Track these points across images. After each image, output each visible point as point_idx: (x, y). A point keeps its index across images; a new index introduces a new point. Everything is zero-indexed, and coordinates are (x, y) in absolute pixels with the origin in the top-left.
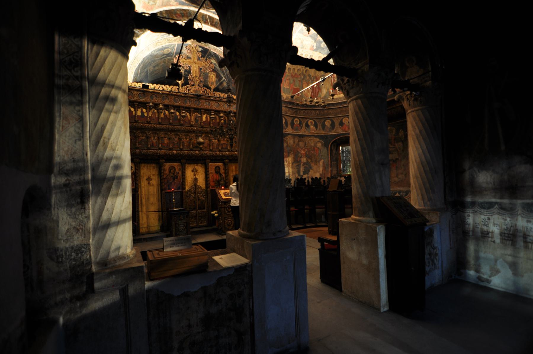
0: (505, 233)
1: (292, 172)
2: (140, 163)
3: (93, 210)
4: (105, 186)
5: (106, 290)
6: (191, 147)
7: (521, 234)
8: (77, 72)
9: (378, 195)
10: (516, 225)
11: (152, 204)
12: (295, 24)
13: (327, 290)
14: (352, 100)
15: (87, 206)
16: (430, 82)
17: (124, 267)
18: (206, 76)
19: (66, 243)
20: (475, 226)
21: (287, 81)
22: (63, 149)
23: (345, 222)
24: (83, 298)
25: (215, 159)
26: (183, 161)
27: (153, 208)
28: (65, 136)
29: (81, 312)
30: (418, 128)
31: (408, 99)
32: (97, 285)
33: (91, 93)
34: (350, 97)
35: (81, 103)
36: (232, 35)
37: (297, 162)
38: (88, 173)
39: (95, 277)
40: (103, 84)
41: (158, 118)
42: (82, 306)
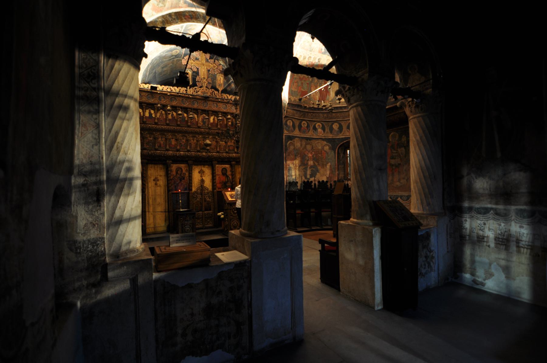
0: (499, 238)
1: (299, 175)
2: (147, 164)
3: (107, 208)
4: (118, 186)
5: (118, 279)
6: (198, 149)
7: (514, 239)
8: (94, 84)
9: (375, 199)
10: (509, 230)
11: (159, 204)
12: (298, 33)
13: (326, 289)
14: (353, 107)
15: (102, 204)
16: (431, 89)
17: (134, 259)
18: (214, 78)
19: (84, 236)
20: (471, 231)
21: (295, 84)
22: (82, 153)
23: (344, 224)
24: (98, 285)
25: (222, 161)
26: (190, 162)
27: (159, 209)
28: (84, 142)
29: (96, 298)
30: (419, 135)
31: (410, 106)
32: (110, 274)
33: (106, 103)
34: (351, 104)
35: (98, 112)
36: (236, 46)
37: (303, 165)
38: (103, 175)
39: (108, 267)
40: (117, 94)
41: (166, 120)
42: (97, 293)
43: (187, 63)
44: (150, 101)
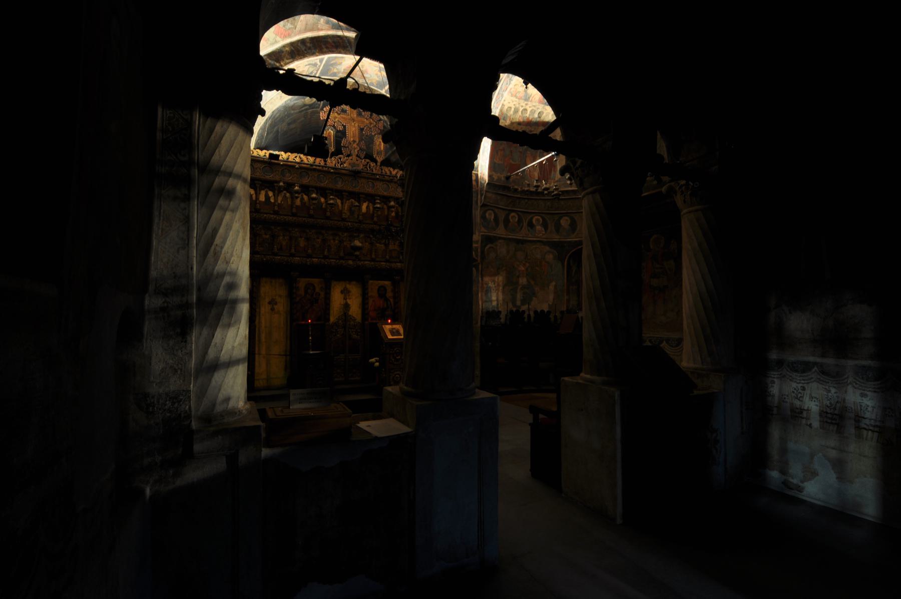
0: (827, 413)
1: (503, 300)
6: (342, 254)
10: (844, 400)
12: (503, 77)
14: (587, 194)
15: (189, 338)
18: (370, 141)
32: (197, 447)
34: (584, 189)
35: (187, 199)
36: (402, 98)
37: (511, 284)
40: (217, 171)
43: (328, 117)
44: (268, 177)
